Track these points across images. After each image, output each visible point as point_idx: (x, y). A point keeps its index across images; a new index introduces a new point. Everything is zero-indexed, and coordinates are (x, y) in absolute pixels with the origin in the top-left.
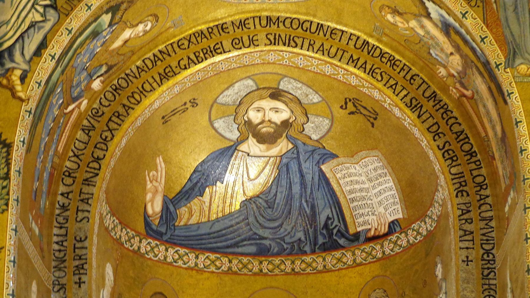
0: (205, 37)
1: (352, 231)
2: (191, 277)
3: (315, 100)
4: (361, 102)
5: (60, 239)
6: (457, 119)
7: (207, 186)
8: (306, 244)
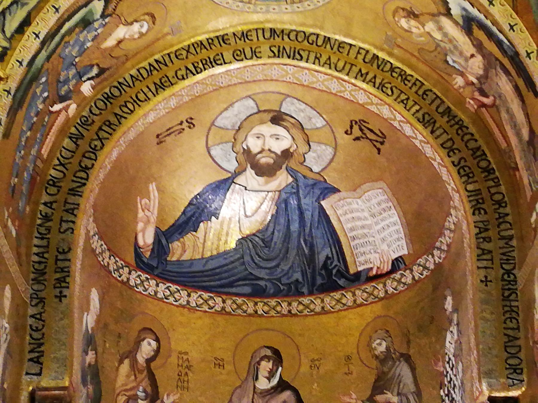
0: (205, 48)
1: (352, 271)
2: (182, 315)
3: (319, 125)
4: (368, 123)
5: (41, 250)
6: (472, 135)
7: (202, 221)
8: (304, 286)
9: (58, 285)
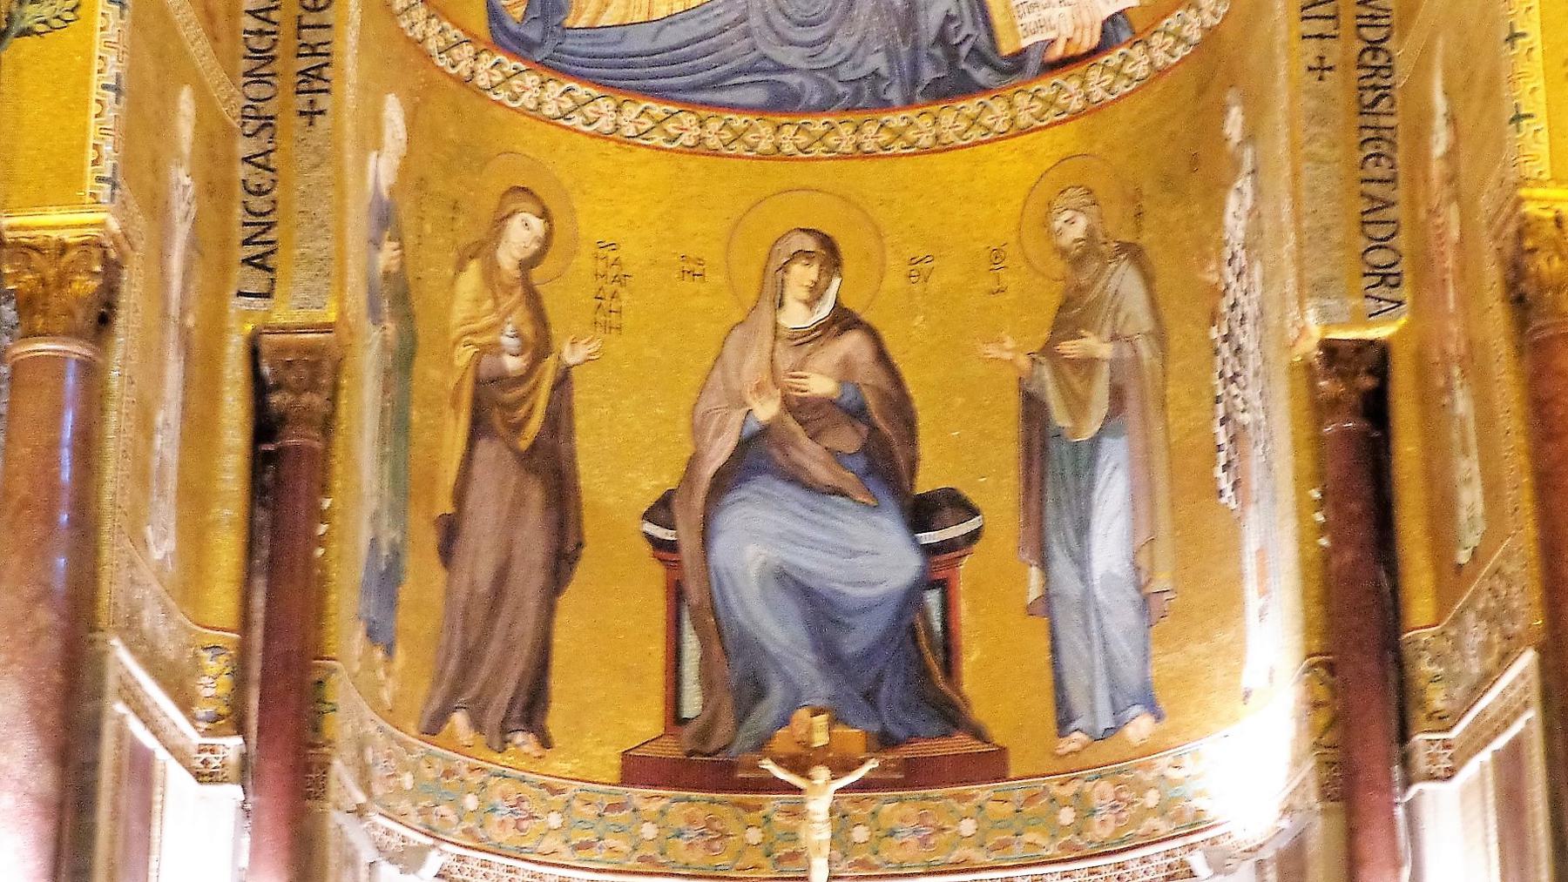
1: (1007, 48)
2: (603, 155)
9: (305, 86)
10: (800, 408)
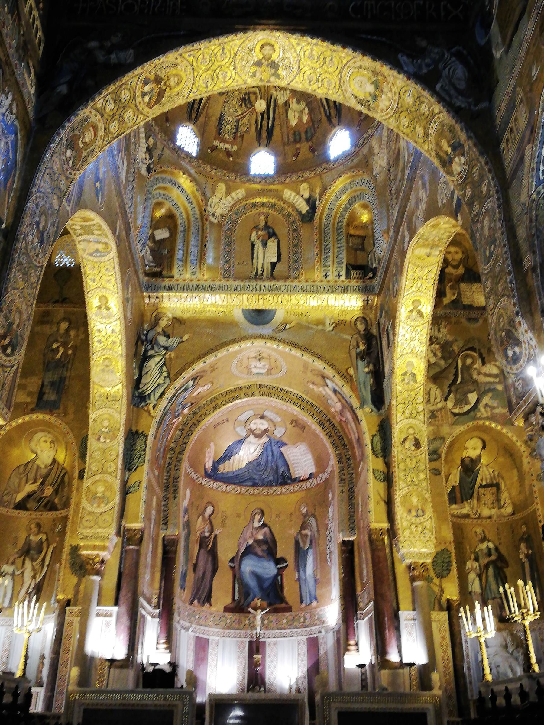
1: (293, 477)
10: (257, 541)
